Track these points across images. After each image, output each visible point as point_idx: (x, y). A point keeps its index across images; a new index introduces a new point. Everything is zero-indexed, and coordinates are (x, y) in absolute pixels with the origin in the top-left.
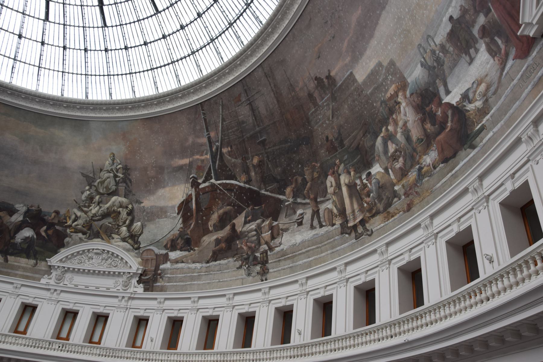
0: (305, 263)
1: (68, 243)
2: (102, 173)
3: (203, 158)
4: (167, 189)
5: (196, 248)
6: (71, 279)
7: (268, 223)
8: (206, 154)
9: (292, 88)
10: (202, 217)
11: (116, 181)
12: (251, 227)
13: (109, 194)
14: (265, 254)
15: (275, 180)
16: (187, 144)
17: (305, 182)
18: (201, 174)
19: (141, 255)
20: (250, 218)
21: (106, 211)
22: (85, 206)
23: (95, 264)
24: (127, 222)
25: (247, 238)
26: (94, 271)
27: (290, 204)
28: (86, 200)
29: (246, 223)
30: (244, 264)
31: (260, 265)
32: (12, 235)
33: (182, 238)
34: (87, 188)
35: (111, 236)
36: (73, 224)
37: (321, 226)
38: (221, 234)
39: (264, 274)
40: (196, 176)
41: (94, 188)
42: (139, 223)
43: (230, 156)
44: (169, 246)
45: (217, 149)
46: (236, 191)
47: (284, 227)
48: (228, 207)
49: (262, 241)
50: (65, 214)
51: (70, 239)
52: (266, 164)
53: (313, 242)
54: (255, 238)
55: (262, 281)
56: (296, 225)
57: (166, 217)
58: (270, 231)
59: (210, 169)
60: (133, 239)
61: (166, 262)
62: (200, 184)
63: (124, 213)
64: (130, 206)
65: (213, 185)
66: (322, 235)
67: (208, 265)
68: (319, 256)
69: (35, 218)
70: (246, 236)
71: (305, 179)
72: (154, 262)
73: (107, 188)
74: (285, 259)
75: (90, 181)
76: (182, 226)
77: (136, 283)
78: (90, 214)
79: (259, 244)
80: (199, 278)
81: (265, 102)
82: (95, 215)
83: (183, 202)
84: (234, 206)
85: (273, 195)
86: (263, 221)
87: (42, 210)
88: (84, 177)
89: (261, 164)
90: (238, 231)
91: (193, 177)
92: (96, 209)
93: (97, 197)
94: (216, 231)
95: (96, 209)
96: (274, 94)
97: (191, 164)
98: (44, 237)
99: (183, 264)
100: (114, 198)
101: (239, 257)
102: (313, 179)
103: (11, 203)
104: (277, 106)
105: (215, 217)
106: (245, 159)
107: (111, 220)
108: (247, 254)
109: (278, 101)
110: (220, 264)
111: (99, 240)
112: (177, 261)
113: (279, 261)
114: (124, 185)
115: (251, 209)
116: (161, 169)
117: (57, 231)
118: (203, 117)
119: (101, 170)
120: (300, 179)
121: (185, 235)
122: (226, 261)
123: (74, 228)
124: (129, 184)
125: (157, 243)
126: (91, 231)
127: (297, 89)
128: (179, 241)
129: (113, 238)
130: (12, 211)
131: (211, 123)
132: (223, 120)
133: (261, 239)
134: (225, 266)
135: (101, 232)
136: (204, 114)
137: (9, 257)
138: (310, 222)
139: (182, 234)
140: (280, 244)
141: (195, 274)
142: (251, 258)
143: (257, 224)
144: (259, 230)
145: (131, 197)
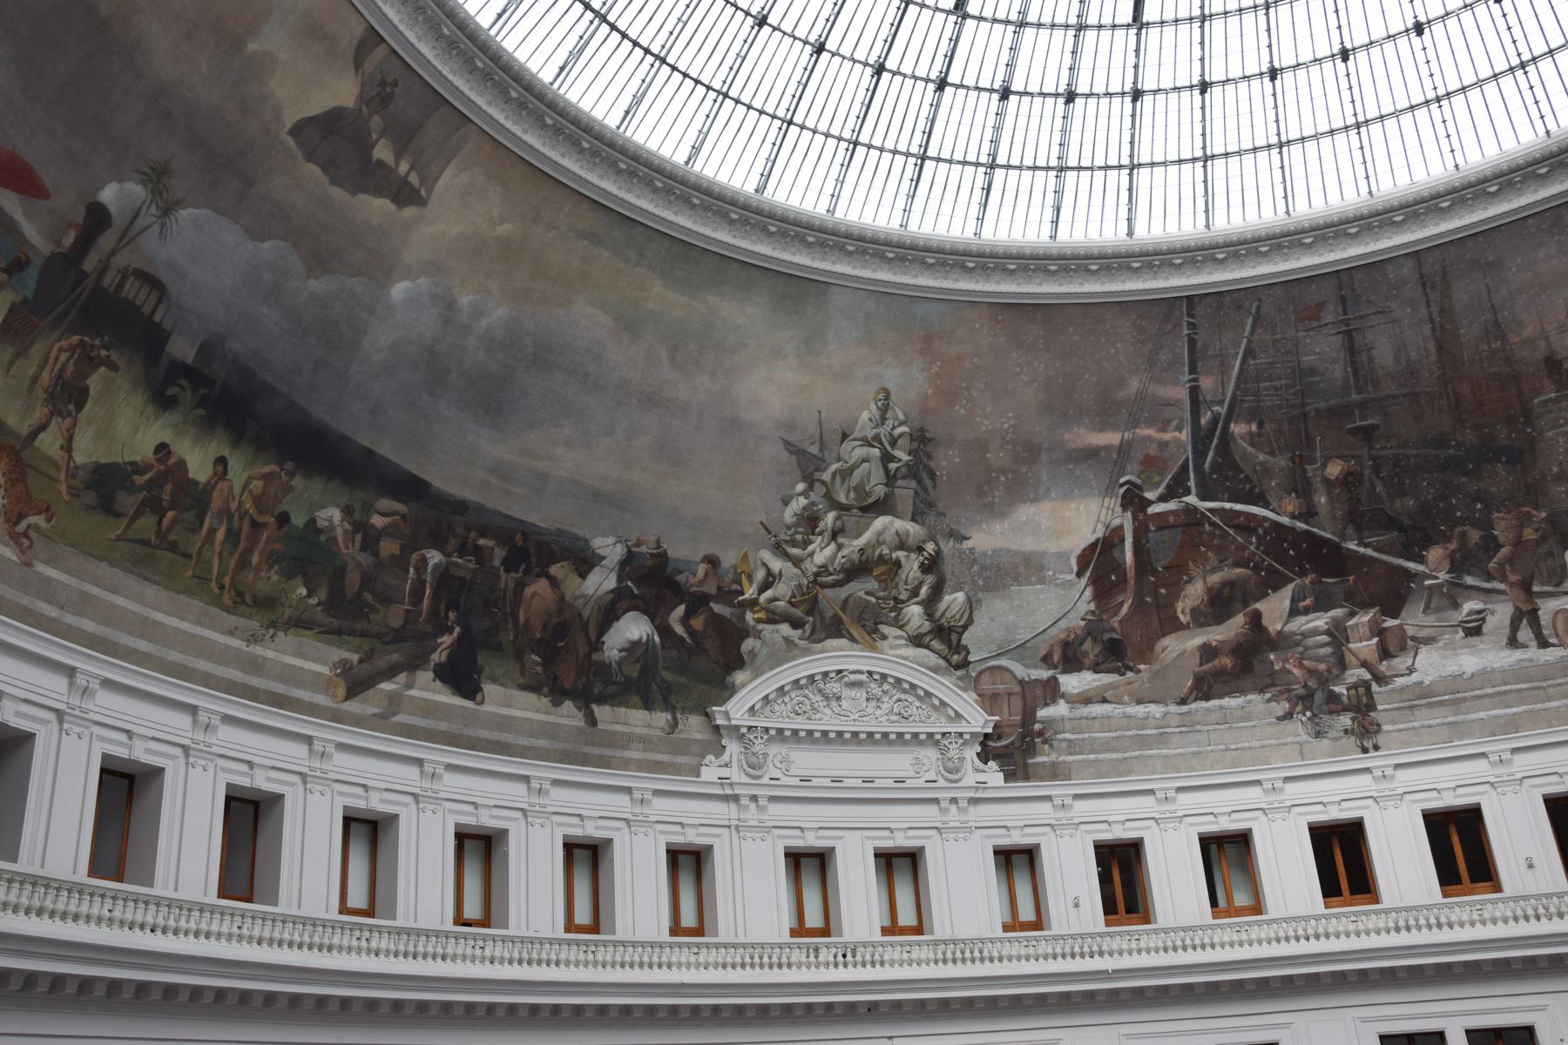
0: (1497, 717)
1: (752, 653)
2: (847, 446)
3: (1166, 436)
4: (1046, 506)
5: (1142, 667)
6: (785, 760)
7: (1366, 618)
8: (1179, 429)
9: (1497, 330)
10: (1156, 587)
11: (887, 471)
12: (1312, 625)
13: (864, 509)
14: (1361, 690)
15: (1391, 523)
16: (1121, 394)
17: (1491, 545)
18: (1157, 478)
19: (974, 684)
20: (1308, 602)
21: (856, 557)
22: (794, 543)
23: (855, 712)
24: (924, 591)
25: (1300, 649)
26: (855, 734)
27: (1439, 586)
28: (797, 525)
29: (1294, 612)
30: (1299, 708)
31: (1350, 715)
32: (593, 638)
33: (1095, 640)
34: (801, 487)
35: (876, 631)
36: (763, 598)
37: (1543, 644)
38: (1217, 634)
39: (1366, 733)
40: (1139, 481)
41: (820, 490)
42: (960, 596)
43: (1252, 445)
44: (1056, 658)
45: (1215, 420)
46: (1265, 533)
47: (1424, 633)
48: (1238, 570)
49: (1349, 658)
50: (735, 567)
51: (758, 643)
52: (1367, 483)
53: (1517, 674)
54: (1328, 650)
55: (1365, 751)
56: (1461, 634)
57: (1042, 581)
58: (1375, 640)
59: (1184, 468)
60: (946, 639)
61: (1054, 701)
62: (1150, 503)
63: (911, 567)
64: (930, 547)
65: (1190, 510)
66: (1547, 664)
67: (1185, 708)
68: (1539, 706)
69: (651, 582)
70: (1298, 644)
71: (1495, 538)
72: (1017, 703)
73: (859, 489)
74: (1430, 705)
75: (809, 466)
76: (1092, 606)
77: (977, 761)
78: (810, 567)
79: (1342, 665)
80: (1162, 739)
81: (1399, 340)
82: (823, 570)
83: (1093, 546)
84: (1256, 569)
85: (1384, 557)
86: (1352, 614)
87: (669, 553)
88: (791, 452)
89: (1349, 481)
90: (1271, 629)
91: (1128, 482)
92: (828, 551)
93: (830, 517)
94: (1201, 625)
95: (828, 551)
96: (1434, 329)
97: (1124, 450)
98: (681, 638)
99: (1107, 707)
100: (881, 522)
101: (1281, 693)
102: (1518, 543)
103: (580, 532)
104: (1433, 358)
105: (1194, 593)
106: (1300, 461)
107: (873, 584)
108: (1305, 686)
109: (1440, 349)
110: (1221, 707)
111: (843, 642)
112: (1086, 699)
113: (1411, 707)
114: (913, 484)
115: (1312, 583)
116: (1029, 452)
117: (716, 619)
118: (1186, 332)
119: (845, 436)
120: (1475, 536)
121: (1105, 631)
122: (1238, 701)
123: (767, 611)
124: (929, 484)
125: (1019, 650)
126: (817, 617)
127: (1514, 339)
128: (1088, 645)
129: (884, 637)
130: (585, 562)
131: (1210, 352)
132: (1250, 353)
133: (1347, 654)
134: (1239, 713)
135: (845, 618)
136: (1191, 326)
137: (594, 707)
138: (1507, 631)
139: (1093, 629)
140: (1411, 670)
141: (1149, 732)
142: (1319, 697)
143: (1333, 618)
144: (1338, 635)
145: (931, 520)
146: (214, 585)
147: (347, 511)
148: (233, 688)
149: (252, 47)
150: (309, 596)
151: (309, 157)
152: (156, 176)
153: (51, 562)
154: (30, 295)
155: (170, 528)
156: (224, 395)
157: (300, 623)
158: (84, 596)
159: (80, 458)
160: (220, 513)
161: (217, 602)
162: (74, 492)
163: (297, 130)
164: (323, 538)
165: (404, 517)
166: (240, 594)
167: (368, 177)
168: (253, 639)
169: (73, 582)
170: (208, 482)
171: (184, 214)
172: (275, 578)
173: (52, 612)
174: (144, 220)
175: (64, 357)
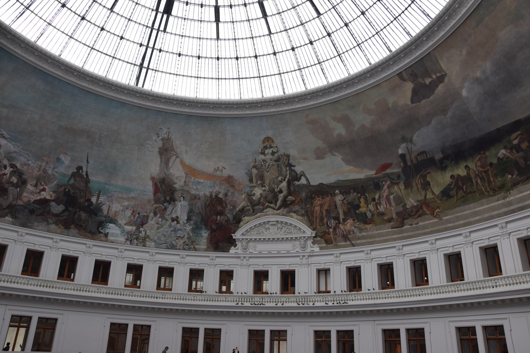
146: (486, 193)
147: (505, 148)
148: (506, 214)
149: (390, 106)
150: (512, 176)
151: (420, 101)
152: (404, 140)
153: (445, 216)
154: (405, 178)
155: (466, 190)
156: (456, 154)
157: (515, 185)
158: (457, 217)
159: (437, 193)
160: (476, 177)
161: (489, 196)
162: (441, 200)
163: (412, 102)
164: (505, 160)
165: (521, 134)
166: (494, 190)
167: (432, 88)
168: (504, 198)
169: (453, 216)
170: (467, 173)
171: (414, 138)
172: (500, 179)
173: (452, 225)
174: (409, 148)
175: (419, 181)
